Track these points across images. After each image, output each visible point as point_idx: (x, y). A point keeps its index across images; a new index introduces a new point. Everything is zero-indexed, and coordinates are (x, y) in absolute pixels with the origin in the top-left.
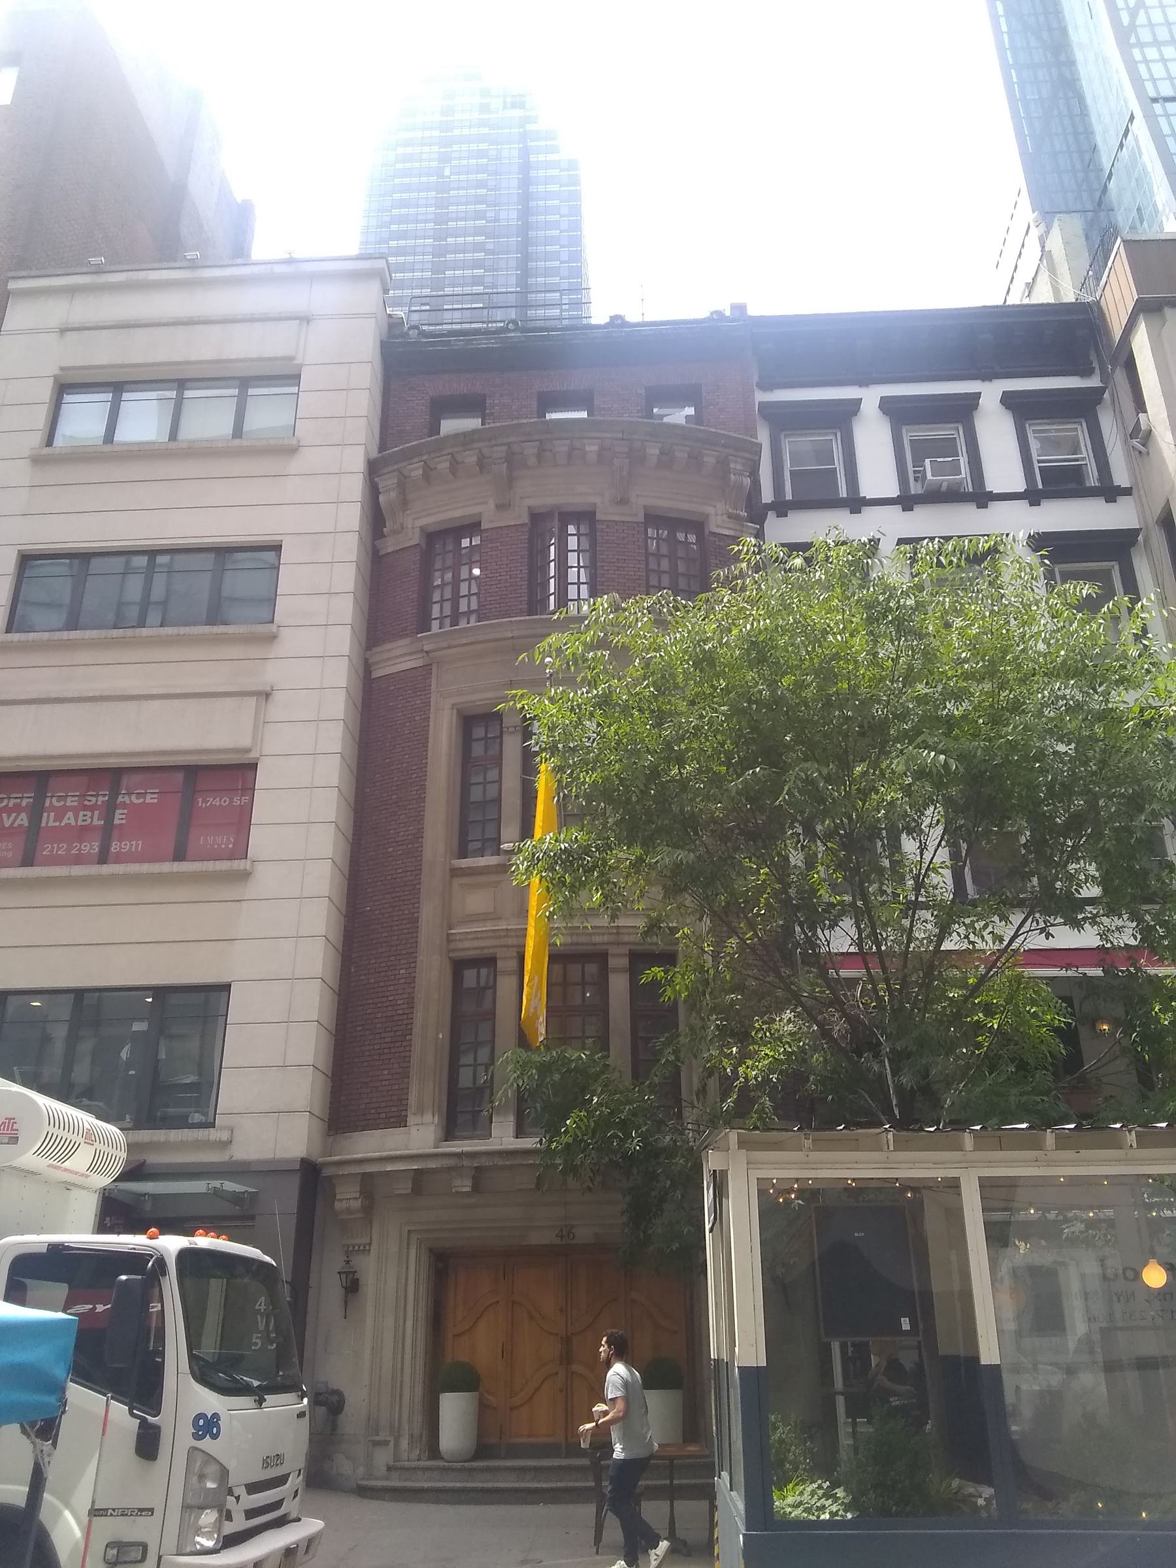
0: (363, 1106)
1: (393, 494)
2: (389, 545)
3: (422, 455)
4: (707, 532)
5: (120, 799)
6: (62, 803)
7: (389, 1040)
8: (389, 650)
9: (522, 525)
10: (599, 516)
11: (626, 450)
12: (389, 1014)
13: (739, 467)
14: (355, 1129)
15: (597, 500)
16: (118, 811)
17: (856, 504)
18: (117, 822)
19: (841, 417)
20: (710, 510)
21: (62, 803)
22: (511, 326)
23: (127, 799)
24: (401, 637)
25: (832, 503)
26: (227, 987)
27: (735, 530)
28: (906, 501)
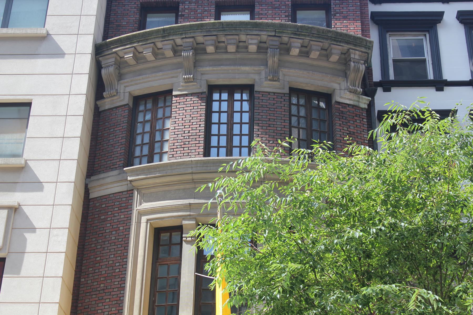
1: (111, 69)
2: (107, 104)
3: (134, 43)
4: (333, 102)
8: (103, 178)
9: (202, 93)
10: (256, 89)
11: (278, 43)
13: (357, 57)
15: (256, 77)
17: (440, 84)
20: (336, 86)
24: (112, 169)
27: (354, 100)
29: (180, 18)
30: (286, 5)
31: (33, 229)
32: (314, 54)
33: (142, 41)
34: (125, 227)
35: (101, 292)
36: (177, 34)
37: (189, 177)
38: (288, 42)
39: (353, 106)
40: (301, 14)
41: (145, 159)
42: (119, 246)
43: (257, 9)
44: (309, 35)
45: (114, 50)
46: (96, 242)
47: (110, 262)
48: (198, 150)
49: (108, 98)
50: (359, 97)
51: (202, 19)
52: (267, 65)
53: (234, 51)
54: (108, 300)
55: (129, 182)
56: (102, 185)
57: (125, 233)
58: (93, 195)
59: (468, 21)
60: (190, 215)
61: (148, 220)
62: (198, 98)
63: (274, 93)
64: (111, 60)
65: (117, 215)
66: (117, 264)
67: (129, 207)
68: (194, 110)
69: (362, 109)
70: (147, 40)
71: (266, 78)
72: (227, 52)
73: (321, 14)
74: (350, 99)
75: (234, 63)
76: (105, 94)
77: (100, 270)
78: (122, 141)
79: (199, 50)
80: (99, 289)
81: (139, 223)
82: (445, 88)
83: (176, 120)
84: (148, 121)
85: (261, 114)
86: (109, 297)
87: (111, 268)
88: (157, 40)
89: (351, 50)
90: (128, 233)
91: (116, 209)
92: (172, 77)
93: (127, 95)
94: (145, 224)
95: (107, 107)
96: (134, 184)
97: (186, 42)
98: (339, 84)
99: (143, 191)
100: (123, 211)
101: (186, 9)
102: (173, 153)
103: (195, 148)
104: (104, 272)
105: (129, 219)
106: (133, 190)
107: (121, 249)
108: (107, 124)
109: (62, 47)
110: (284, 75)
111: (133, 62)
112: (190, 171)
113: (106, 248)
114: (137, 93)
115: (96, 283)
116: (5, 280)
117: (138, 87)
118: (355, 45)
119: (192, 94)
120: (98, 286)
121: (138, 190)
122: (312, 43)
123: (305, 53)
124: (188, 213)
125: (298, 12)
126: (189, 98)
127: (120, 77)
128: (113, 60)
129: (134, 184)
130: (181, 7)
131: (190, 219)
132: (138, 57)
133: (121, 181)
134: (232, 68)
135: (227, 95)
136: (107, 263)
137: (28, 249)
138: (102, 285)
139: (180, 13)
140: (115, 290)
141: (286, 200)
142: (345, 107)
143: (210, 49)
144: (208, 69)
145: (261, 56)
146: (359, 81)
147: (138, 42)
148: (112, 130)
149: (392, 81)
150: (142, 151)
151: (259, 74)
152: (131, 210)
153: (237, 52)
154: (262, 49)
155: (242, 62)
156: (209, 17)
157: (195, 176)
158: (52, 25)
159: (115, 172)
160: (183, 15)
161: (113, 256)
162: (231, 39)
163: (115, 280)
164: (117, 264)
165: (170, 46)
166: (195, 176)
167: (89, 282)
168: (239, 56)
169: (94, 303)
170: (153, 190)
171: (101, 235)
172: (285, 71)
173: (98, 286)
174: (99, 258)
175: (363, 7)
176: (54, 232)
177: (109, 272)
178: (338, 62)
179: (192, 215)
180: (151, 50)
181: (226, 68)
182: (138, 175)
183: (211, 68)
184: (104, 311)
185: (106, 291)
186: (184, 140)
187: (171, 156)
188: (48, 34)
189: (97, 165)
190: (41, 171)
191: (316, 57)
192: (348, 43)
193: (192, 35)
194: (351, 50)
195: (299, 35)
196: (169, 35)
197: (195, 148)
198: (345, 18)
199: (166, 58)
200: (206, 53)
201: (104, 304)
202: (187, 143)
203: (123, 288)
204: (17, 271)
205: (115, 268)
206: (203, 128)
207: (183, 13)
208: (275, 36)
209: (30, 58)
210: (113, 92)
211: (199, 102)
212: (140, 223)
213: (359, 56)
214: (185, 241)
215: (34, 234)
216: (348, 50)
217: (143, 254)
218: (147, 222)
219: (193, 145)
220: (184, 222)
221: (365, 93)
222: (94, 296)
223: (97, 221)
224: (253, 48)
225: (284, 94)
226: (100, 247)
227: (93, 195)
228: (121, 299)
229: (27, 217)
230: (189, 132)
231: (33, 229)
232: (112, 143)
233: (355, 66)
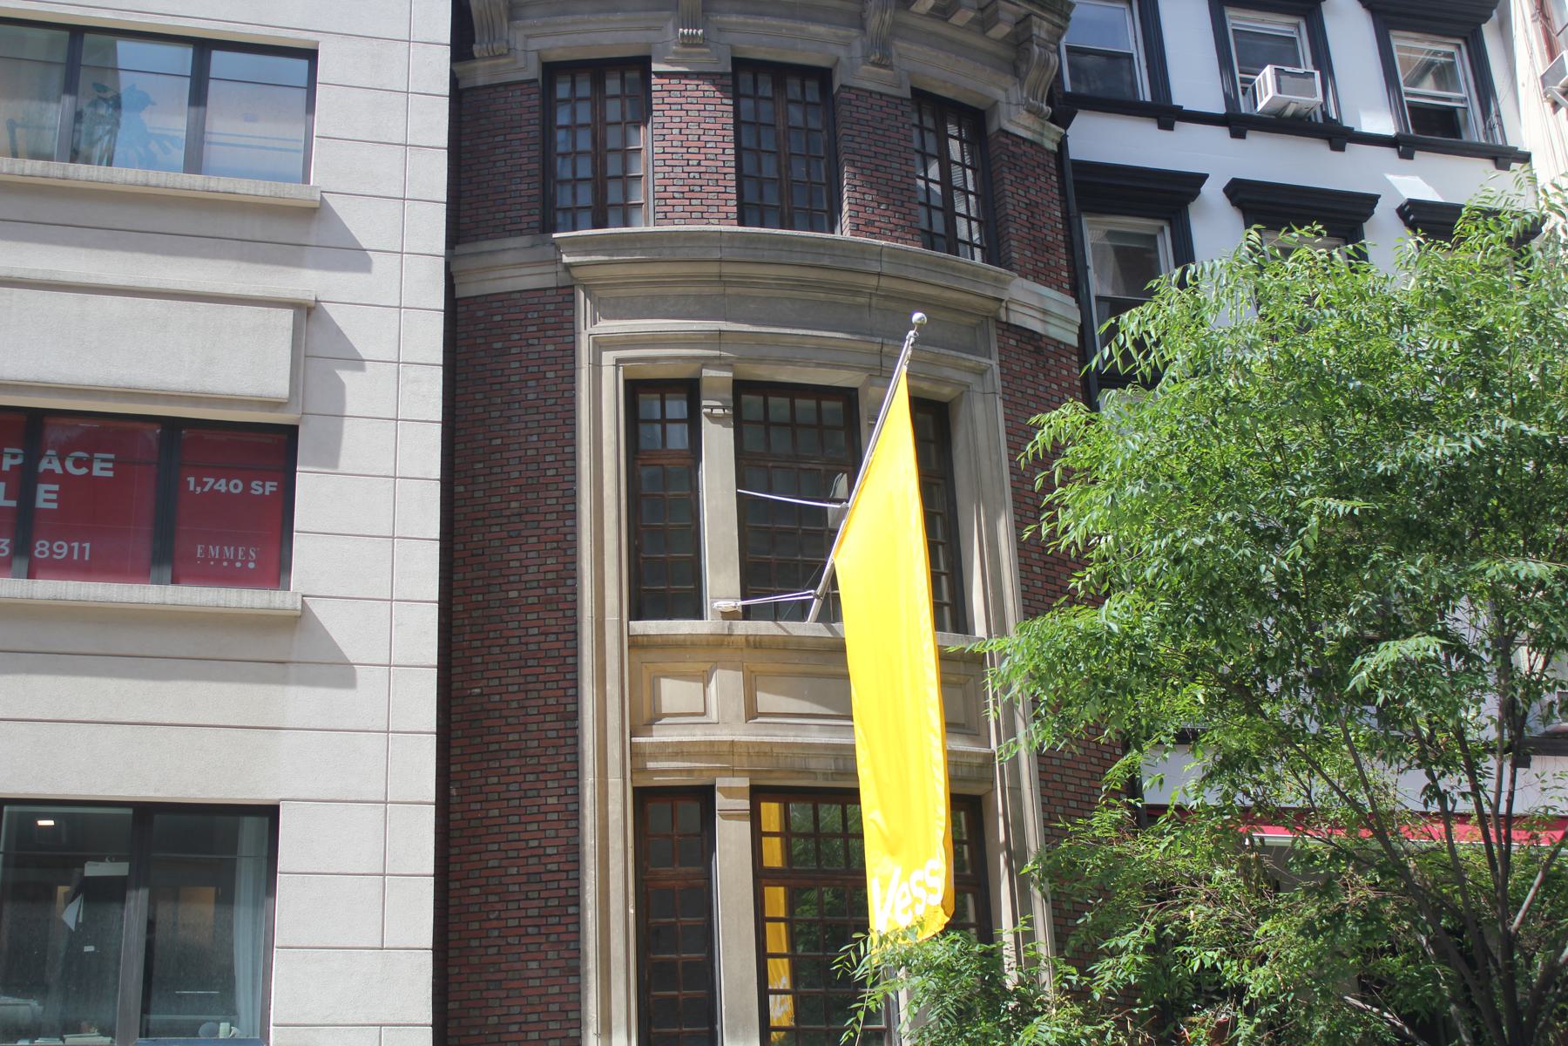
2: (481, 73)
5: (44, 465)
6: (84, 471)
7: (535, 912)
8: (491, 252)
9: (722, 75)
12: (531, 869)
13: (1043, 35)
15: (842, 53)
16: (42, 488)
17: (1166, 115)
18: (40, 504)
20: (999, 94)
21: (84, 471)
23: (56, 467)
24: (511, 233)
25: (1125, 106)
26: (269, 814)
27: (1034, 132)
28: (1237, 123)
31: (357, 362)
32: (963, 17)
34: (560, 373)
37: (713, 269)
39: (1032, 143)
41: (586, 217)
46: (486, 402)
47: (530, 453)
49: (483, 58)
52: (862, 27)
54: (534, 540)
55: (560, 268)
57: (561, 387)
58: (461, 292)
60: (720, 357)
61: (618, 361)
63: (881, 94)
66: (549, 458)
67: (567, 325)
69: (1049, 152)
71: (866, 58)
74: (1027, 128)
76: (476, 48)
78: (531, 167)
80: (508, 512)
81: (597, 366)
82: (1178, 124)
84: (582, 126)
87: (534, 466)
89: (1034, 18)
92: (648, 29)
93: (533, 57)
95: (481, 80)
96: (575, 272)
98: (1006, 90)
99: (598, 293)
100: (550, 333)
104: (516, 474)
105: (571, 353)
108: (482, 122)
110: (900, 55)
112: (717, 255)
113: (515, 419)
114: (555, 56)
117: (561, 41)
118: (1042, 8)
119: (699, 75)
120: (504, 505)
121: (585, 288)
124: (717, 353)
126: (691, 85)
129: (575, 272)
133: (541, 263)
134: (789, 24)
135: (770, 86)
136: (522, 453)
137: (351, 408)
138: (514, 504)
140: (549, 517)
142: (1016, 145)
144: (734, 19)
146: (1043, 91)
149: (1144, 103)
150: (574, 196)
151: (848, 45)
152: (573, 333)
157: (728, 269)
161: (535, 438)
163: (549, 494)
164: (549, 458)
166: (728, 269)
170: (622, 292)
172: (900, 46)
173: (504, 505)
174: (498, 441)
176: (411, 372)
177: (529, 474)
178: (1003, 41)
181: (774, 22)
183: (741, 19)
184: (526, 562)
185: (527, 518)
187: (661, 215)
189: (467, 220)
190: (362, 222)
191: (960, 23)
194: (1034, 18)
201: (525, 548)
203: (573, 515)
204: (329, 458)
210: (499, 46)
213: (1048, 32)
215: (359, 374)
216: (1028, 16)
217: (614, 438)
218: (617, 366)
220: (707, 373)
221: (1053, 120)
225: (902, 99)
227: (461, 292)
228: (569, 537)
229: (339, 332)
231: (357, 362)
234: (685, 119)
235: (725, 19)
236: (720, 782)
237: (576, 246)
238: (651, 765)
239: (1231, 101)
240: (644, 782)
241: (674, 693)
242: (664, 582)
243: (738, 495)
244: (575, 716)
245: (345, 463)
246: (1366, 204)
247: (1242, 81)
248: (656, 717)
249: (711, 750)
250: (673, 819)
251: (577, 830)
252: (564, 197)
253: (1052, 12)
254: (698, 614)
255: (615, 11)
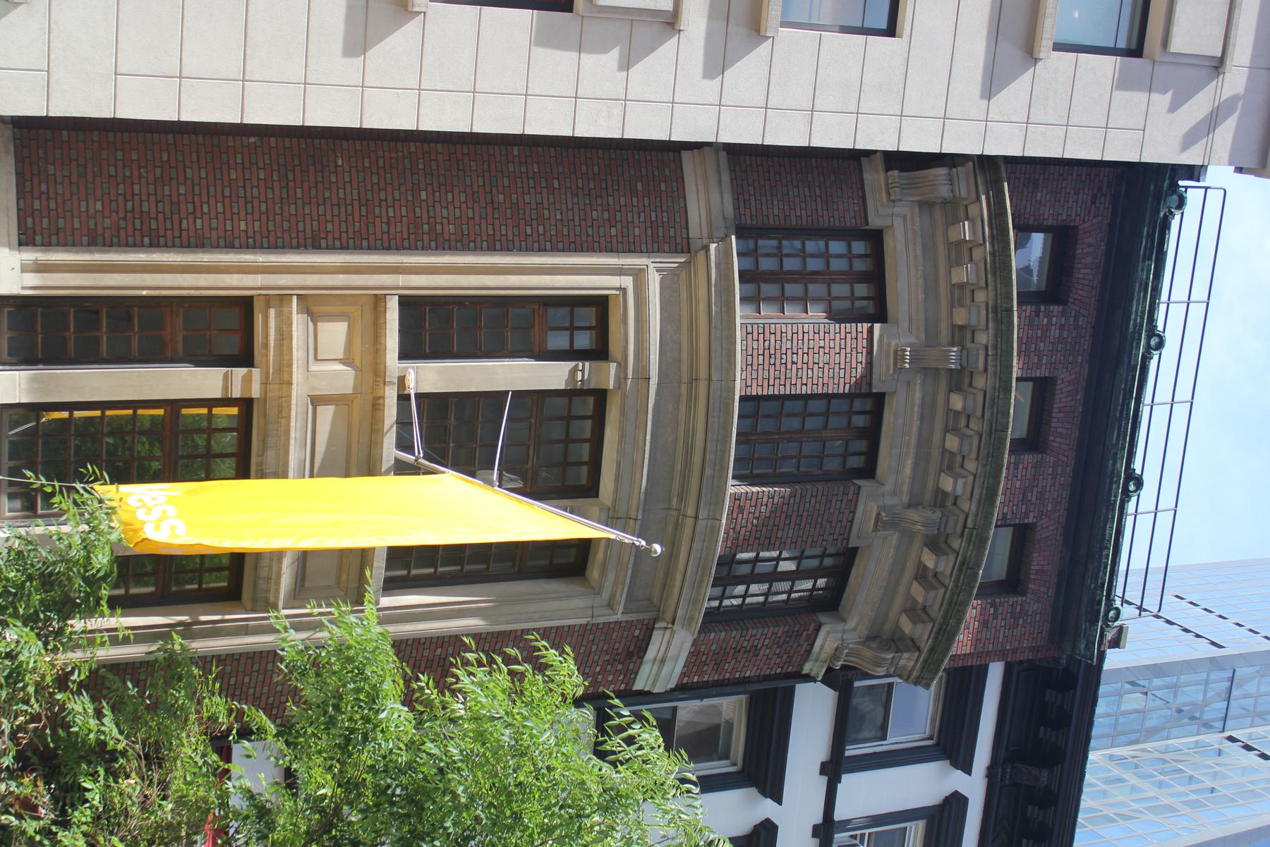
0: (51, 169)
1: (944, 191)
2: (874, 177)
3: (992, 243)
4: (822, 618)
7: (145, 208)
9: (870, 384)
11: (949, 531)
12: (183, 207)
13: (902, 662)
14: (19, 160)
15: (888, 488)
17: (834, 769)
19: (951, 744)
20: (851, 624)
22: (1153, 342)
24: (736, 199)
25: (842, 732)
27: (819, 653)
29: (1034, 308)
30: (1026, 514)
31: (626, 64)
32: (918, 592)
33: (993, 261)
34: (614, 240)
35: (489, 196)
36: (996, 336)
37: (703, 374)
38: (950, 547)
39: (809, 652)
40: (1006, 535)
42: (578, 228)
43: (1028, 458)
44: (957, 586)
45: (983, 197)
47: (546, 212)
48: (754, 385)
49: (887, 179)
50: (825, 661)
51: (1004, 494)
52: (910, 506)
53: (947, 445)
54: (470, 214)
55: (705, 241)
56: (706, 181)
57: (602, 240)
58: (686, 155)
59: (946, 814)
60: (626, 378)
61: (624, 290)
62: (862, 377)
63: (852, 521)
64: (963, 190)
65: (642, 219)
66: (541, 228)
68: (837, 370)
69: (801, 666)
70: (994, 274)
71: (883, 508)
72: (946, 430)
73: (1000, 570)
74: (822, 647)
75: (924, 443)
76: (895, 173)
77: (532, 191)
79: (958, 380)
81: (621, 271)
82: (825, 779)
83: (822, 334)
85: (813, 500)
86: (477, 218)
88: (991, 294)
89: (916, 654)
90: (603, 246)
91: (653, 215)
92: (910, 321)
93: (888, 222)
94: (618, 285)
95: (867, 177)
96: (701, 254)
97: (977, 355)
98: (855, 629)
99: (684, 274)
100: (649, 232)
101: (1050, 319)
102: (755, 333)
103: (760, 378)
104: (527, 200)
106: (689, 252)
107: (572, 235)
109: (1004, 92)
111: (953, 237)
112: (714, 377)
113: (575, 200)
115: (506, 184)
116: (524, 18)
118: (925, 662)
119: (870, 364)
121: (688, 262)
122: (942, 591)
123: (923, 576)
125: (1030, 384)
126: (862, 358)
127: (926, 206)
128: (964, 194)
129: (701, 254)
130: (1056, 309)
131: (618, 378)
132: (959, 251)
134: (913, 442)
135: (861, 425)
137: (587, 59)
138: (501, 197)
139: (1043, 308)
140: (490, 227)
141: (629, 725)
142: (807, 639)
143: (957, 402)
144: (918, 395)
145: (928, 496)
146: (854, 661)
147: (993, 254)
148: (818, 193)
149: (844, 750)
152: (649, 251)
153: (944, 450)
154: (941, 499)
155: (921, 459)
156: (1026, 366)
157: (702, 386)
158: (1055, 65)
159: (729, 210)
160: (1038, 315)
161: (559, 217)
162: (971, 444)
163: (510, 227)
164: (541, 228)
165: (974, 322)
166: (702, 386)
167: (511, 165)
168: (936, 453)
169: (468, 182)
170: (684, 294)
171: (604, 185)
172: (894, 538)
173: (501, 189)
174: (556, 185)
175: (1000, 655)
176: (617, 110)
177: (528, 211)
178: (897, 628)
179: (626, 383)
180: (973, 280)
181: (915, 429)
182: (717, 266)
183: (918, 401)
184: (451, 207)
185: (490, 209)
186: (778, 355)
187: (750, 329)
188: (1036, 60)
190: (747, 72)
191: (912, 591)
192: (932, 650)
193: (990, 369)
194: (916, 654)
195: (960, 570)
196: (998, 322)
197: (760, 378)
198: (984, 624)
199: (952, 306)
200: (951, 390)
201: (464, 206)
202: (772, 361)
203: (492, 248)
204: (543, 39)
205: (535, 225)
206: (798, 392)
207: (1042, 314)
208: (965, 526)
209: (990, 26)
211: (853, 380)
212: (620, 275)
213: (904, 667)
214: (576, 366)
215: (616, 65)
216: (918, 649)
217: (557, 285)
218: (620, 289)
219: (766, 373)
220: (613, 366)
221: (829, 670)
222: (480, 180)
223: (632, 172)
224: (947, 484)
225: (848, 539)
226: (580, 185)
227: (686, 155)
228: (472, 244)
230: (793, 363)
231: (626, 64)
232: (791, 194)
233: (885, 659)
234: (832, 352)
235: (918, 387)
236: (256, 372)
237: (724, 256)
238: (272, 312)
239: (845, 825)
240: (257, 306)
241: (334, 334)
242: (434, 326)
243: (507, 392)
244: (316, 247)
245: (539, 52)
246: (774, 790)
247: (863, 835)
248: (314, 317)
249: (284, 365)
250: (225, 331)
251: (216, 246)
252: (767, 244)
253: (922, 670)
254: (403, 356)
255: (926, 293)
